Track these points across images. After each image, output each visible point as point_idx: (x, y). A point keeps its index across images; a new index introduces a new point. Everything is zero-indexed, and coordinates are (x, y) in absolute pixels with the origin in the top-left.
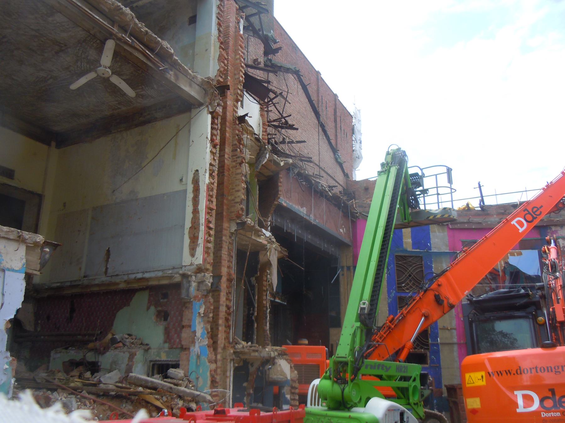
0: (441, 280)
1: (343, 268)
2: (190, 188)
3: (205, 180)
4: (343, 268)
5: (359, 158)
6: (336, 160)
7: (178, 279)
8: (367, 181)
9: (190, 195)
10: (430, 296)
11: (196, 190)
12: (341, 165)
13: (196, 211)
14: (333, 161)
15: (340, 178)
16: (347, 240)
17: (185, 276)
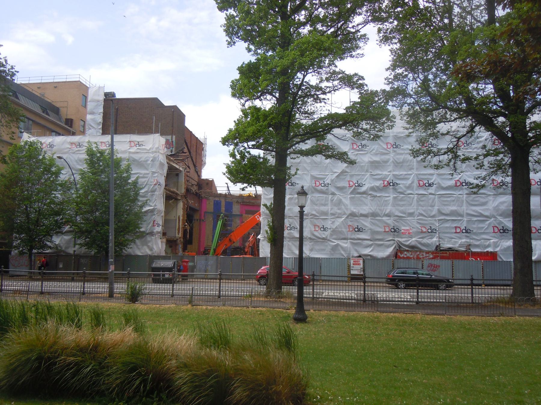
0: (232, 234)
1: (195, 220)
2: (178, 219)
3: (181, 218)
4: (195, 220)
5: (205, 163)
6: (195, 170)
7: (175, 239)
8: (207, 180)
9: (177, 221)
10: (228, 239)
11: (179, 220)
12: (197, 172)
13: (179, 225)
14: (194, 171)
15: (196, 178)
16: (197, 208)
17: (177, 239)
